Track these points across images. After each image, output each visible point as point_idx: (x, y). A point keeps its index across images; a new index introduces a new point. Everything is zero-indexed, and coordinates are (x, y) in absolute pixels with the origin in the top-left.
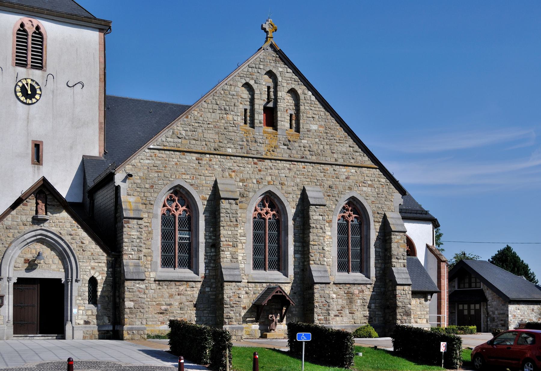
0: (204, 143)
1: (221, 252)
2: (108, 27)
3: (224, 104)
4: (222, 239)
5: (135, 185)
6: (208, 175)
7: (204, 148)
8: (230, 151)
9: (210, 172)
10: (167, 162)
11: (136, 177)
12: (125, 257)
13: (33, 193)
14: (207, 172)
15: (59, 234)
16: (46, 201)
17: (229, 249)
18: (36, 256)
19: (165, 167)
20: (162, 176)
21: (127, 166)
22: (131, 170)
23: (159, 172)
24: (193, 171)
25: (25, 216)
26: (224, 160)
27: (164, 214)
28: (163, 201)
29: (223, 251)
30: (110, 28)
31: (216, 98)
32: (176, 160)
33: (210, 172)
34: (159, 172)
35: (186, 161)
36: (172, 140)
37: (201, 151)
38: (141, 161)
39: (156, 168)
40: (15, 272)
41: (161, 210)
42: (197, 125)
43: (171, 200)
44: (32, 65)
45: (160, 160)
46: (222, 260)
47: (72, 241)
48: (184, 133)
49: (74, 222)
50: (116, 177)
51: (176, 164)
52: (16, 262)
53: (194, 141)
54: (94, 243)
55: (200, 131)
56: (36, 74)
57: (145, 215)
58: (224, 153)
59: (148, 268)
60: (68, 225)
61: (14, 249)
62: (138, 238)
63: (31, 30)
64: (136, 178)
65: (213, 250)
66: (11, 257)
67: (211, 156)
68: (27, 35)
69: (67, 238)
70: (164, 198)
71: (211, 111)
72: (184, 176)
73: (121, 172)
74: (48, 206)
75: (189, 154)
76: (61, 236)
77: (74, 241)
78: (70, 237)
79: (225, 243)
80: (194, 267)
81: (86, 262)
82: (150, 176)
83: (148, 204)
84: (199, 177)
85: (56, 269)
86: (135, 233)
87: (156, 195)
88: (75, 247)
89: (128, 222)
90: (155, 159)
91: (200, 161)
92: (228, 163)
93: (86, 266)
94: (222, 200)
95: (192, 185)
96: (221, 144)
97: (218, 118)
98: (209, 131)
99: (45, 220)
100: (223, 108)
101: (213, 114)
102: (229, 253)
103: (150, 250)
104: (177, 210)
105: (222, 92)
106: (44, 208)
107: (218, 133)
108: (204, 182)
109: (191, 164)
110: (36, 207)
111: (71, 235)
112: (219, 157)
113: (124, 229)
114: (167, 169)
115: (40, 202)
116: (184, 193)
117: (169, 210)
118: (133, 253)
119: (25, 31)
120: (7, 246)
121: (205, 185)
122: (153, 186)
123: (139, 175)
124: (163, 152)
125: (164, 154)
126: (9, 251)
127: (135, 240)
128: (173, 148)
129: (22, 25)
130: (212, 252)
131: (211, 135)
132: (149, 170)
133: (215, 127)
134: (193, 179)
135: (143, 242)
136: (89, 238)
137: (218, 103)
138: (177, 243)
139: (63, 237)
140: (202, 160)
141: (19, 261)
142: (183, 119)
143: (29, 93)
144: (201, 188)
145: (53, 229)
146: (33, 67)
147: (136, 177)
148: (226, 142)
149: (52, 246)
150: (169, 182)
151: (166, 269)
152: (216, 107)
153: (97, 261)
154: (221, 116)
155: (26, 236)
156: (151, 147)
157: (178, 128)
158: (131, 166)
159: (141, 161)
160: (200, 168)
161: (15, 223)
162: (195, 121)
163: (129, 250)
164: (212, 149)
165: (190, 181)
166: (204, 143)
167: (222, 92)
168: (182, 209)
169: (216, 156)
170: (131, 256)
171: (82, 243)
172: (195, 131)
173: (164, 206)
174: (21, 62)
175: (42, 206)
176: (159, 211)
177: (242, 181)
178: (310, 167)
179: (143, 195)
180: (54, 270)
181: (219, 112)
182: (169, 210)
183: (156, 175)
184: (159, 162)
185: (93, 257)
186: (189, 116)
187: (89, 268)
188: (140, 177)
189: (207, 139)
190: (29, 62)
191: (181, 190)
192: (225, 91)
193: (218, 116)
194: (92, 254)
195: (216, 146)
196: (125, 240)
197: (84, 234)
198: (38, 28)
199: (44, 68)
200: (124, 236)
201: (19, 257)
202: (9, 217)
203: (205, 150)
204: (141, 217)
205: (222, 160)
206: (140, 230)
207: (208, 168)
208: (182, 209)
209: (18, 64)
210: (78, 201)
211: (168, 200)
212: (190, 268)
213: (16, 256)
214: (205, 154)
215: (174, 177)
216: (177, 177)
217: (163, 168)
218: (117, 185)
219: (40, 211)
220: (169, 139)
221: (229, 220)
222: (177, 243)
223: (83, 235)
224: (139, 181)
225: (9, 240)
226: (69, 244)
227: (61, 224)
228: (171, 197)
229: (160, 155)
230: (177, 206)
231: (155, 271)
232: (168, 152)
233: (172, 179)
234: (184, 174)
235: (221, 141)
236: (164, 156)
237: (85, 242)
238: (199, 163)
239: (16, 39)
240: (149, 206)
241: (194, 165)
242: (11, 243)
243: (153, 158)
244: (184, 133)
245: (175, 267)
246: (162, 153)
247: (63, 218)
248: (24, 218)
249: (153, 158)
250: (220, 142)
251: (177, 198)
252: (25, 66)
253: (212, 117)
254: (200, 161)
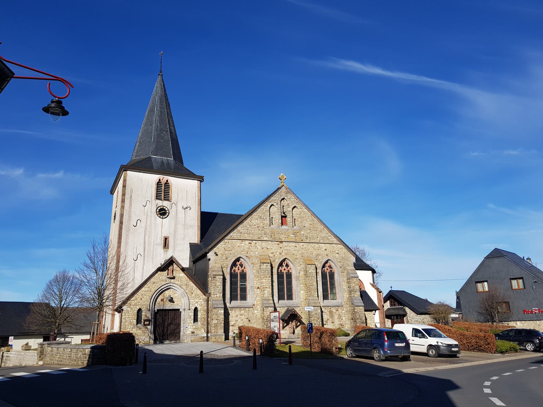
8: (265, 239)
56: (166, 204)
63: (163, 182)
92: (264, 244)
143: (162, 212)
174: (158, 197)
177: (272, 253)
178: (305, 245)
197: (193, 285)
252: (161, 199)
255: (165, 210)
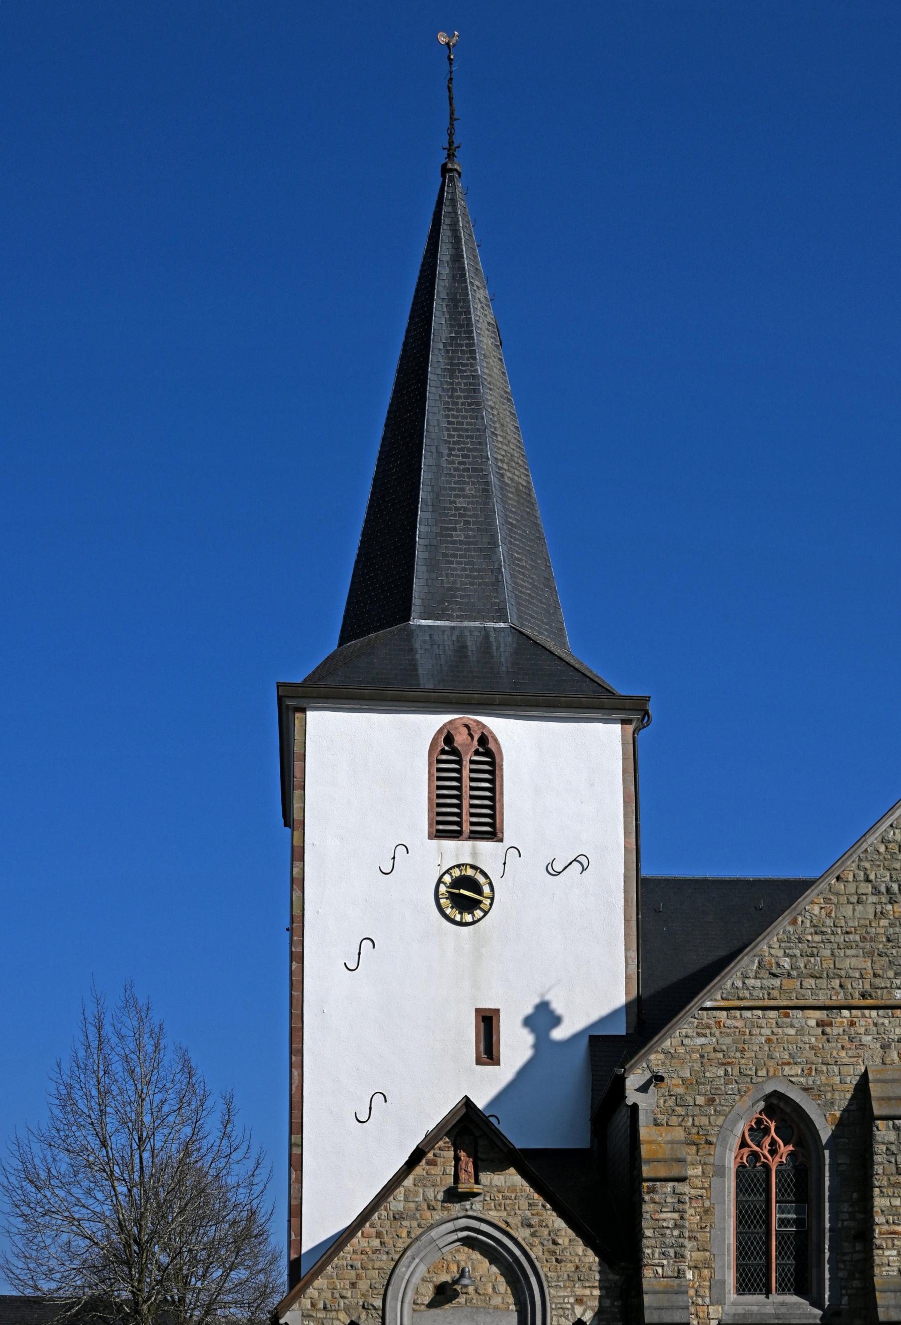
0: (836, 983)
1: (876, 1252)
2: (643, 713)
3: (888, 878)
4: (879, 1219)
5: (671, 1102)
6: (846, 1060)
7: (837, 994)
9: (850, 1053)
10: (747, 1037)
11: (674, 1082)
12: (647, 1273)
14: (843, 1054)
15: (504, 1226)
16: (476, 1152)
17: (896, 1242)
18: (458, 1276)
19: (743, 1051)
20: (736, 1072)
21: (653, 1057)
22: (663, 1064)
23: (728, 1064)
24: (811, 1055)
25: (432, 1190)
26: (886, 1022)
27: (742, 1166)
28: (739, 1134)
29: (880, 1247)
30: (646, 713)
31: (867, 865)
32: (768, 1032)
33: (850, 1053)
34: (728, 1064)
35: (792, 1032)
36: (758, 983)
37: (828, 1003)
38: (687, 1041)
39: (720, 1055)
40: (415, 1315)
41: (733, 1155)
42: (817, 938)
43: (758, 1130)
44: (472, 832)
45: (729, 1035)
46: (877, 1271)
47: (531, 1240)
48: (786, 963)
49: (536, 1196)
50: (628, 1083)
51: (769, 1041)
52: (417, 1292)
53: (812, 981)
54: (581, 1242)
55: (828, 953)
57: (694, 1171)
58: (889, 1003)
59: (703, 1297)
60: (524, 1204)
61: (411, 1263)
62: (676, 1226)
64: (673, 1082)
65: (859, 1246)
66: (405, 1281)
67: (854, 1012)
68: (459, 762)
69: (522, 1234)
70: (741, 1127)
71: (854, 899)
72: (787, 1070)
73: (640, 1071)
74: (479, 1163)
75: (799, 1013)
76: (508, 1229)
77: (537, 1240)
78: (527, 1232)
79: (885, 1228)
80: (814, 1291)
81: (565, 1287)
82: (707, 1074)
83: (701, 1141)
84: (824, 1068)
85: (501, 1306)
86: (669, 1217)
87: (720, 1120)
88: (540, 1254)
89: (652, 1190)
90: (717, 1033)
91: (828, 1030)
93: (564, 1297)
94: (878, 1122)
95: (806, 1090)
96: (877, 981)
97: (871, 917)
98: (849, 952)
99: (470, 1195)
100: (883, 889)
101: (859, 908)
102: (895, 1253)
103: (708, 1254)
104: (773, 1152)
105: (882, 849)
106: (471, 1169)
107: (870, 954)
108: (837, 1079)
109: (806, 1039)
110: (456, 1166)
111: (530, 1226)
112: (874, 1013)
113: (645, 1208)
114: (747, 1054)
115: (462, 1154)
116: (788, 1110)
117: (755, 1156)
118: (665, 1262)
119: (454, 752)
120: (397, 1257)
121: (839, 1087)
122: (713, 1100)
123: (681, 1074)
124: (737, 1013)
125: (736, 1021)
126: (401, 1269)
127: (668, 1232)
128: (760, 1003)
130: (856, 1252)
131: (854, 962)
132: (705, 1061)
133: (863, 939)
134: (810, 1075)
135: (687, 1234)
136: (570, 1231)
137: (872, 877)
138: (774, 1233)
139: (512, 1232)
140: (830, 1024)
141: (422, 1290)
142: (783, 926)
144: (829, 1096)
145: (493, 1215)
146: (475, 836)
147: (674, 1082)
148: (891, 974)
149: (492, 1254)
150: (751, 1086)
151: (742, 1297)
152: (867, 888)
153: (587, 1285)
154: (879, 908)
155: (434, 1233)
156: (708, 1004)
157: (772, 951)
158: (662, 1056)
159: (687, 1041)
160: (827, 1046)
161: (412, 1205)
162: (812, 930)
163: (657, 1255)
164: (857, 995)
165: (802, 1080)
166: (837, 981)
167: (882, 849)
168: (785, 1150)
169: (867, 1012)
170: (660, 1270)
171: (555, 1243)
172: (812, 955)
173: (743, 1144)
176: (731, 1159)
179: (690, 1123)
180: (496, 1308)
181: (874, 899)
182: (755, 1156)
183: (721, 1072)
184: (728, 1040)
185: (578, 1275)
186: (800, 919)
187: (572, 1300)
188: (683, 1080)
189: (843, 973)
190: (466, 828)
191: (782, 1105)
192: (890, 846)
193: (871, 910)
194: (577, 1267)
195: (867, 986)
196: (648, 1233)
197: (560, 1223)
198: (483, 740)
199: (499, 835)
200: (644, 1224)
201: (424, 1280)
203: (840, 998)
204: (683, 1174)
205: (881, 1021)
206: (681, 1207)
207: (847, 1044)
208: (785, 1150)
209: (439, 835)
210: (585, 1147)
211: (751, 1129)
212: (800, 1291)
213: (416, 1279)
214: (840, 1008)
215: (762, 1073)
216: (771, 1074)
217: (738, 1055)
218: (630, 1103)
219: (463, 1176)
220: (751, 982)
221: (894, 1171)
222: (774, 1233)
223: (556, 1225)
224: (681, 1090)
225: (401, 1245)
226: (527, 1248)
227: (508, 1202)
228: (759, 1121)
229: (729, 1022)
230: (773, 1143)
231: (720, 1302)
232: (748, 1014)
233: (760, 1080)
234: (789, 1064)
235: (880, 972)
236: (739, 1024)
237: (560, 1241)
238: (823, 1033)
239: (436, 774)
240: (704, 1149)
241: (813, 1040)
242: (405, 1250)
243: (714, 1030)
244: (786, 963)
245: (768, 1293)
246: (735, 1018)
247: (512, 1189)
249: (714, 1030)
250: (875, 975)
251: (773, 1126)
253: (857, 914)
254: (828, 1030)
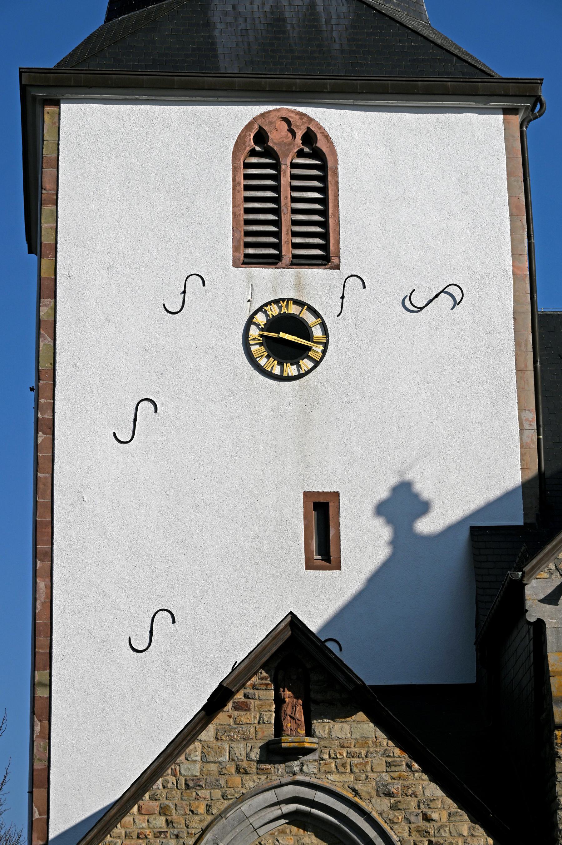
13: (264, 667)
15: (350, 795)
25: (242, 745)
44: (294, 256)
49: (397, 751)
54: (466, 817)
60: (379, 763)
68: (276, 166)
69: (377, 807)
74: (313, 707)
76: (357, 799)
77: (400, 816)
78: (386, 803)
88: (406, 835)
106: (300, 715)
110: (278, 712)
111: (389, 794)
115: (287, 694)
119: (269, 152)
129: (261, 137)
136: (449, 801)
139: (363, 804)
145: (333, 780)
146: (299, 261)
155: (245, 807)
161: (214, 768)
171: (427, 818)
175: (295, 707)
190: (287, 252)
197: (434, 790)
198: (309, 138)
199: (334, 260)
202: (195, 750)
219: (288, 725)
223: (428, 794)
226: (386, 827)
227: (356, 760)
237: (435, 816)
242: (204, 832)
247: (363, 742)
248: (240, 750)
255: (303, 330)
